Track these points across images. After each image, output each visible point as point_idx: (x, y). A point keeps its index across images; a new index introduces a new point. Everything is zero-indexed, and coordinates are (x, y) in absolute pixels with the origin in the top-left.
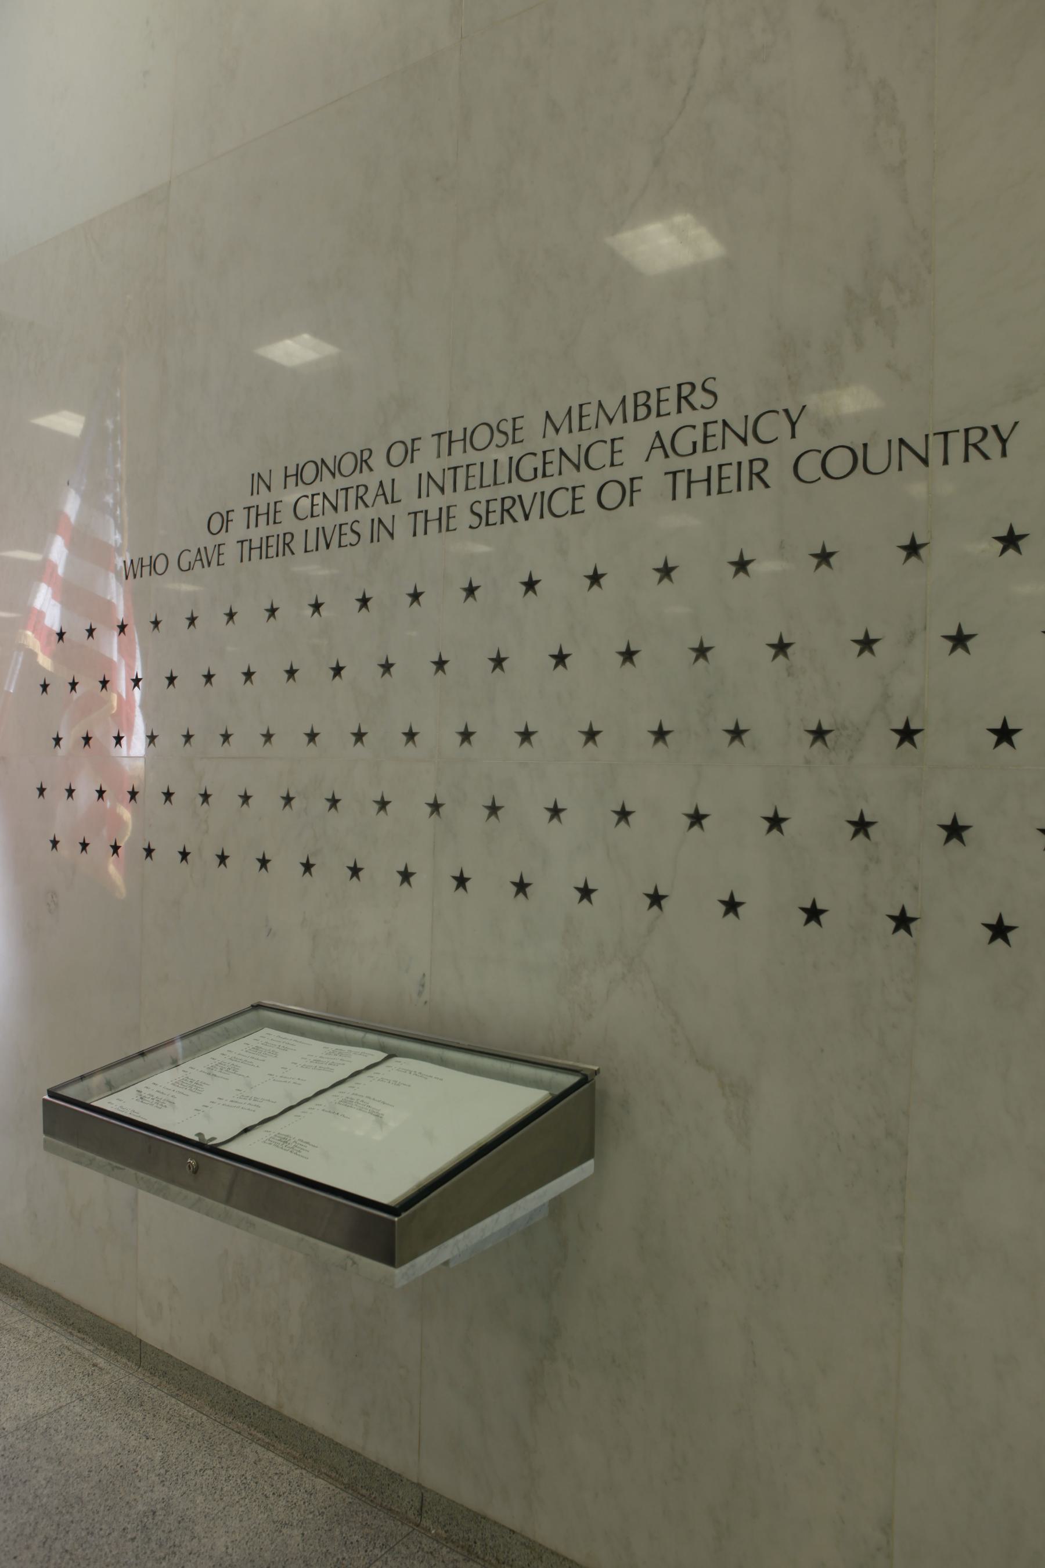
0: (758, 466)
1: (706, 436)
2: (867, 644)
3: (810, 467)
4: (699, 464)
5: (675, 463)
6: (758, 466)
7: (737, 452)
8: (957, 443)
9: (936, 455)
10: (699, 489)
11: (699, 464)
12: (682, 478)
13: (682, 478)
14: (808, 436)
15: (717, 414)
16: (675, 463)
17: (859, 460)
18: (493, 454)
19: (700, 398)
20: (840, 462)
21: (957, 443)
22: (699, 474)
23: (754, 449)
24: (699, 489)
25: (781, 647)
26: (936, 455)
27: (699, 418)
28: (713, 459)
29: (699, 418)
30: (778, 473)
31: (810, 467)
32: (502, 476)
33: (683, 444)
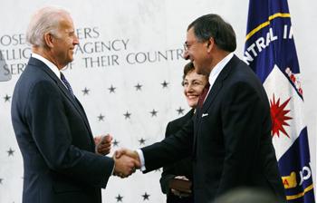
0: (115, 58)
1: (96, 47)
2: (154, 113)
3: (132, 59)
4: (95, 56)
5: (86, 55)
6: (115, 58)
7: (107, 53)
8: (175, 53)
9: (169, 58)
10: (95, 64)
11: (95, 56)
12: (89, 61)
13: (89, 61)
14: (130, 49)
15: (100, 39)
16: (86, 55)
17: (147, 57)
18: (10, 48)
19: (92, 33)
20: (141, 58)
21: (175, 53)
22: (95, 59)
23: (113, 52)
24: (95, 64)
25: (128, 115)
26: (169, 58)
27: (93, 41)
28: (99, 55)
29: (93, 41)
30: (121, 60)
31: (132, 59)
32: (17, 55)
33: (88, 48)
